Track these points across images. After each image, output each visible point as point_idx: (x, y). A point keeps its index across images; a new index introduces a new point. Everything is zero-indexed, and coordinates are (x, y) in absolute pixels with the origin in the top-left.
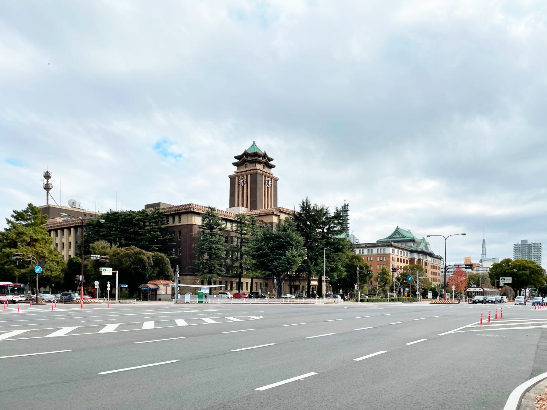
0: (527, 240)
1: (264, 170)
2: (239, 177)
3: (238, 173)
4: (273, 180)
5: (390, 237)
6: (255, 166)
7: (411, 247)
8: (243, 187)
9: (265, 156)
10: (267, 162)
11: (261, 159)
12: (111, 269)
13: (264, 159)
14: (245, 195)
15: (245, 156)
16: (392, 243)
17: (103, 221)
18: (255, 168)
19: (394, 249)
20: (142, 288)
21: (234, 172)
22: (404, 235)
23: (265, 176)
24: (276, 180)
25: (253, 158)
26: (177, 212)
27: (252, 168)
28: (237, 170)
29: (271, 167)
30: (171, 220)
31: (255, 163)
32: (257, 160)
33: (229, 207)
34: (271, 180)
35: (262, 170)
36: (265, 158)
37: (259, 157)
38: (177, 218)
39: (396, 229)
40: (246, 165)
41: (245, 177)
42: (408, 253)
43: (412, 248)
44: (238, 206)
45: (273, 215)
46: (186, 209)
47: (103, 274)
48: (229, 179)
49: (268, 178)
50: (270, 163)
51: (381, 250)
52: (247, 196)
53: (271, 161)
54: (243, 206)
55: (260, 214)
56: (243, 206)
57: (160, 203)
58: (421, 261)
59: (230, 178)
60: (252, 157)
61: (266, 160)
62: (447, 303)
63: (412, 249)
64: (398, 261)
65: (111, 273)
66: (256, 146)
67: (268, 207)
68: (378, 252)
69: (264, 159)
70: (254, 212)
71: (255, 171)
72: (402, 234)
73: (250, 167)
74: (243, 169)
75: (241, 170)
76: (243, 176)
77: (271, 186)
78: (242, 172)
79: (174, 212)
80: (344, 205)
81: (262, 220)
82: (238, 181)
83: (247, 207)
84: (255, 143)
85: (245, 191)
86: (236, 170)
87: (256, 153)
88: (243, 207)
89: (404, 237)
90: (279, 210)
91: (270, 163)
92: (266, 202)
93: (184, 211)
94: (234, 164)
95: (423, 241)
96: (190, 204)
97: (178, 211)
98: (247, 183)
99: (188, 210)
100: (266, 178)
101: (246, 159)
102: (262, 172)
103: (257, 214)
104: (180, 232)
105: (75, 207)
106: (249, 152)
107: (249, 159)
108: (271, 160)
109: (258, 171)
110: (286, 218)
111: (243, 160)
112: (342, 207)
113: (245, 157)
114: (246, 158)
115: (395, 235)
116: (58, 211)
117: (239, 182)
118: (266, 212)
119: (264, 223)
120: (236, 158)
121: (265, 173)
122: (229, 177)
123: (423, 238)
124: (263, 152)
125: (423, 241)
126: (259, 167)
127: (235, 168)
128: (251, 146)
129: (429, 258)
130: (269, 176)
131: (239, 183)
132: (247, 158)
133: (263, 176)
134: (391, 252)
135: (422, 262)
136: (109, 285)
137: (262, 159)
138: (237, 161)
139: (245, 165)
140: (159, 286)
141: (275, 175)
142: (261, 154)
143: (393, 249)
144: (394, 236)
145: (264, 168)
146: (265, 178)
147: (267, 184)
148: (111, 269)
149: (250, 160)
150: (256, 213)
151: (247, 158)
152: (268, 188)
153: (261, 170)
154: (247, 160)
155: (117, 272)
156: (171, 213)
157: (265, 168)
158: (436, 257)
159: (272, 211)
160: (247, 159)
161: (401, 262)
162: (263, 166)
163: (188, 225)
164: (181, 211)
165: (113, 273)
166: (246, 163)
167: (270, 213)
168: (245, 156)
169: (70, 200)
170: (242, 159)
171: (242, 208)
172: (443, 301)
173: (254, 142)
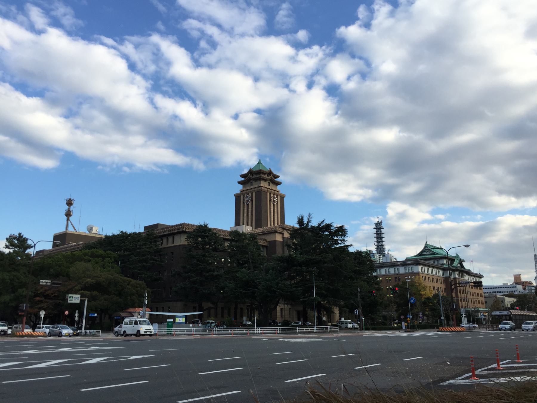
0: (144, 227)
3: (243, 191)
4: (279, 197)
5: (420, 254)
6: (260, 183)
7: (444, 264)
8: (248, 205)
9: (270, 173)
10: (273, 179)
11: (266, 176)
12: (79, 296)
13: (269, 176)
14: (250, 213)
16: (420, 260)
17: (58, 243)
21: (240, 190)
22: (434, 252)
23: (270, 194)
24: (282, 198)
26: (170, 232)
27: (256, 186)
28: (243, 188)
29: (278, 183)
30: (165, 241)
31: (260, 181)
32: (262, 177)
34: (277, 197)
35: (267, 187)
36: (270, 175)
37: (264, 174)
38: (170, 239)
39: (425, 245)
40: (251, 183)
41: (250, 195)
42: (441, 271)
43: (445, 266)
44: (243, 224)
45: (276, 233)
46: (179, 229)
47: (69, 302)
48: (235, 198)
49: (274, 195)
50: (277, 180)
51: (409, 269)
52: (252, 214)
54: (248, 225)
55: (263, 232)
57: (158, 224)
58: (457, 280)
60: (257, 175)
61: (272, 177)
62: (446, 330)
63: (445, 267)
64: (429, 281)
65: (78, 300)
66: (261, 164)
69: (269, 176)
70: (259, 230)
72: (433, 251)
73: (255, 185)
74: (248, 187)
75: (246, 189)
76: (248, 194)
77: (277, 204)
78: (247, 190)
80: (377, 222)
82: (244, 199)
83: (252, 226)
84: (261, 161)
85: (250, 209)
86: (242, 188)
87: (261, 170)
90: (282, 227)
91: (277, 180)
92: (272, 219)
93: (177, 231)
94: (240, 183)
95: (457, 257)
96: (183, 224)
98: (252, 201)
99: (180, 230)
100: (272, 195)
102: (267, 189)
103: (260, 233)
104: (172, 253)
105: (92, 232)
106: (254, 170)
107: (255, 176)
108: (277, 177)
109: (262, 188)
111: (248, 178)
112: (376, 225)
113: (250, 175)
114: (251, 176)
115: (424, 252)
116: (77, 237)
117: (244, 200)
118: (269, 230)
119: (267, 241)
120: (242, 176)
121: (270, 190)
123: (456, 254)
124: (269, 169)
125: (457, 257)
126: (263, 184)
127: (241, 187)
128: (257, 165)
130: (275, 193)
131: (244, 201)
132: (253, 176)
133: (268, 194)
134: (420, 271)
136: (77, 315)
137: (268, 176)
138: (243, 179)
139: (250, 182)
142: (267, 172)
143: (422, 267)
144: (424, 253)
145: (269, 185)
146: (270, 195)
147: (272, 201)
148: (79, 296)
149: (255, 178)
150: (259, 232)
151: (253, 176)
152: (274, 205)
153: (266, 188)
155: (87, 299)
156: (165, 233)
158: (475, 275)
159: (274, 229)
160: (252, 177)
161: (433, 281)
162: (269, 183)
163: (180, 245)
164: (173, 232)
165: (81, 300)
166: (252, 181)
167: (272, 231)
169: (88, 226)
172: (446, 328)
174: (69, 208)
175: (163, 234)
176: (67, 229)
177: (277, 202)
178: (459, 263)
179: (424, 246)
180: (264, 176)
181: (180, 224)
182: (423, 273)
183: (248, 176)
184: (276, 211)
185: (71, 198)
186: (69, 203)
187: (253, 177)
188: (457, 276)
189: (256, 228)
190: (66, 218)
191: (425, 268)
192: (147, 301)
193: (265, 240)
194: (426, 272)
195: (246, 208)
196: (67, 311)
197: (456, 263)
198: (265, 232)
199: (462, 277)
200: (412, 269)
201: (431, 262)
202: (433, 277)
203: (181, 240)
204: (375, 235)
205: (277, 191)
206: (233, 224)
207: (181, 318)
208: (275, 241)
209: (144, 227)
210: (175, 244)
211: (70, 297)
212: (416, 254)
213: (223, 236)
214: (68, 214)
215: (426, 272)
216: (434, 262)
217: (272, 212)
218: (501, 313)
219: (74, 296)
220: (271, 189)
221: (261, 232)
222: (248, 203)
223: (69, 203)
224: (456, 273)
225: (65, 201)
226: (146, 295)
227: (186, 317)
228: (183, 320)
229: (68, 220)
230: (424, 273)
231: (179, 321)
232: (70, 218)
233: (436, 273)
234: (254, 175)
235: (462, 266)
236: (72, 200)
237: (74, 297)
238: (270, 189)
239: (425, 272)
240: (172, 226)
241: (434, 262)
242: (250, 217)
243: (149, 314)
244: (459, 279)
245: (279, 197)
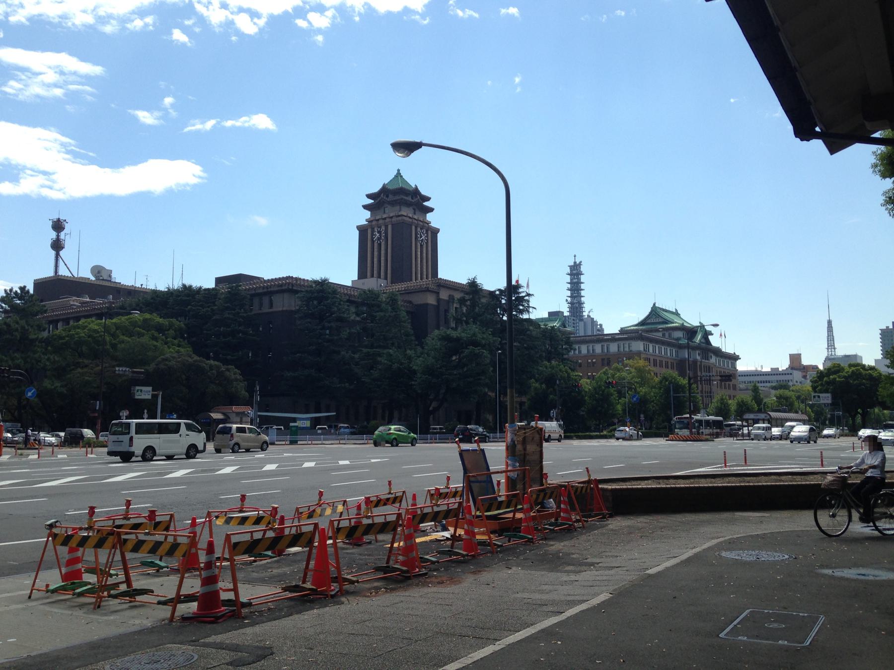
1: (416, 217)
4: (430, 233)
8: (380, 245)
9: (416, 192)
12: (150, 389)
15: (382, 194)
18: (400, 214)
19: (647, 344)
20: (201, 419)
23: (416, 228)
25: (397, 197)
26: (265, 290)
33: (357, 279)
41: (383, 228)
44: (372, 276)
47: (137, 397)
48: (358, 232)
50: (426, 204)
53: (427, 201)
55: (407, 290)
56: (379, 277)
58: (699, 364)
59: (358, 229)
60: (394, 196)
65: (149, 395)
66: (401, 176)
67: (427, 278)
68: (620, 350)
71: (400, 218)
72: (662, 318)
75: (378, 218)
76: (381, 228)
77: (427, 243)
79: (261, 291)
80: (573, 264)
81: (410, 300)
82: (372, 234)
83: (386, 278)
84: (401, 172)
85: (383, 252)
88: (379, 279)
89: (667, 323)
91: (426, 204)
92: (419, 269)
94: (366, 207)
97: (268, 288)
99: (284, 288)
100: (419, 229)
101: (385, 200)
102: (411, 220)
103: (401, 291)
106: (390, 187)
107: (391, 198)
108: (428, 199)
110: (450, 295)
113: (384, 196)
120: (369, 196)
121: (416, 222)
122: (359, 228)
124: (414, 186)
126: (406, 212)
127: (367, 214)
128: (394, 178)
130: (423, 226)
133: (413, 227)
135: (700, 366)
137: (412, 198)
138: (371, 201)
140: (229, 415)
141: (433, 224)
142: (409, 191)
143: (645, 343)
144: (649, 321)
145: (415, 214)
151: (387, 196)
152: (421, 245)
153: (410, 218)
154: (387, 200)
155: (161, 393)
157: (416, 212)
161: (661, 366)
162: (414, 209)
164: (272, 289)
165: (153, 396)
168: (382, 194)
170: (379, 199)
171: (377, 280)
173: (399, 170)
174: (58, 236)
175: (254, 292)
176: (56, 272)
177: (427, 240)
179: (649, 310)
180: (406, 198)
181: (283, 277)
182: (646, 353)
183: (380, 198)
184: (425, 255)
185: (61, 218)
186: (58, 226)
188: (698, 358)
190: (53, 253)
192: (259, 396)
194: (651, 350)
196: (128, 413)
197: (699, 338)
198: (410, 290)
199: (705, 359)
200: (629, 347)
202: (661, 359)
204: (569, 286)
205: (426, 223)
207: (305, 422)
208: (427, 304)
209: (216, 278)
211: (138, 391)
212: (636, 322)
214: (57, 246)
215: (651, 350)
217: (419, 256)
218: (756, 416)
219: (144, 388)
220: (417, 220)
221: (403, 291)
222: (380, 241)
223: (58, 226)
224: (697, 352)
225: (51, 223)
226: (256, 389)
227: (311, 418)
228: (307, 424)
229: (57, 256)
230: (649, 353)
231: (302, 426)
232: (62, 253)
233: (666, 353)
234: (390, 196)
235: (708, 342)
236: (62, 221)
237: (143, 390)
238: (415, 219)
239: (650, 351)
242: (383, 264)
244: (701, 362)
245: (430, 233)
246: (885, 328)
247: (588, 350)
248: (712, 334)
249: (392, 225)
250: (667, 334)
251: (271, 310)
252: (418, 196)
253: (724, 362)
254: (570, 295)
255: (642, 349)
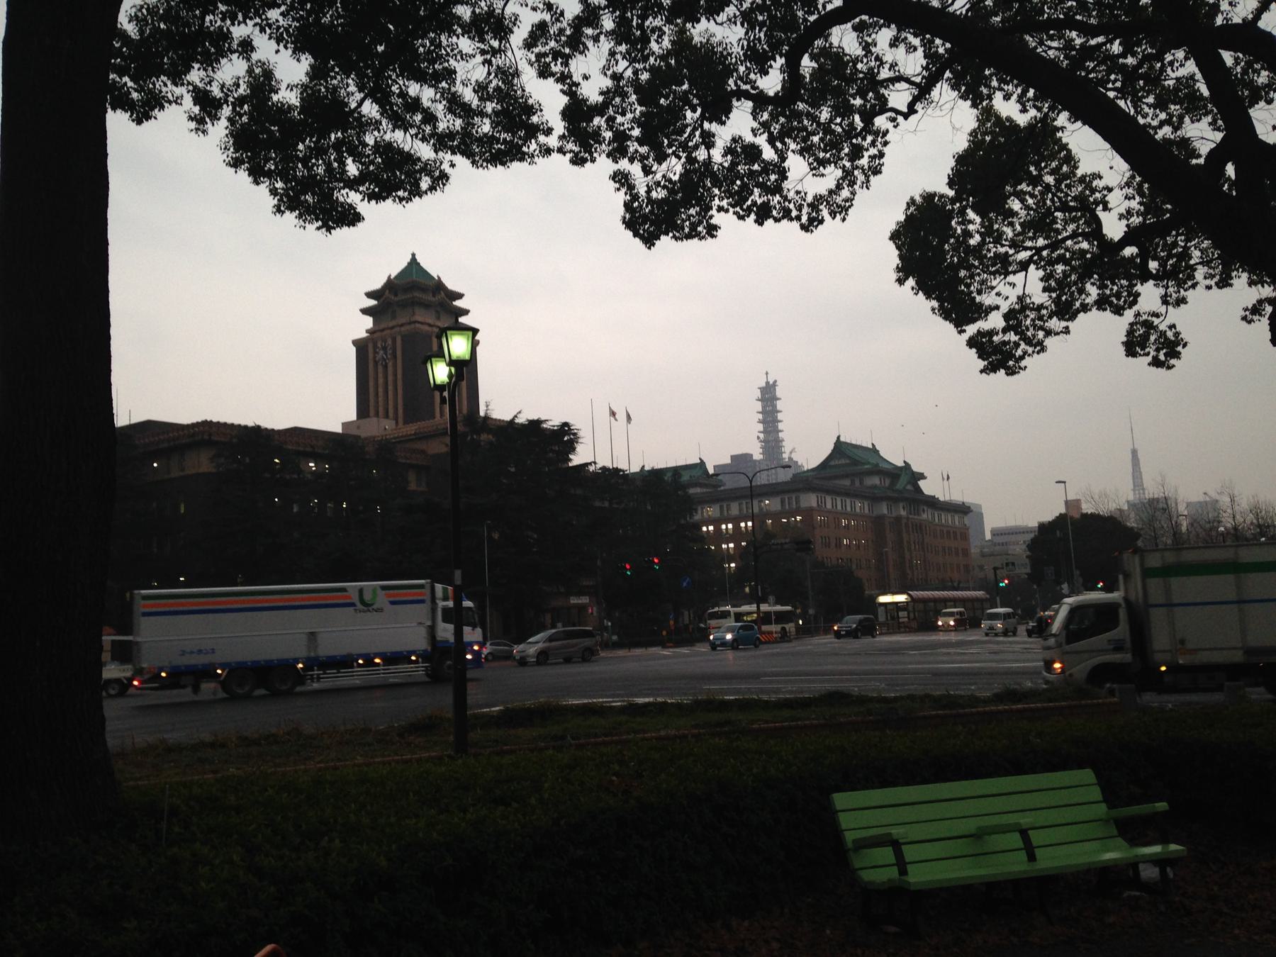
2: (375, 346)
8: (386, 367)
9: (439, 286)
15: (387, 291)
25: (409, 296)
26: (172, 444)
41: (390, 342)
48: (354, 349)
50: (458, 303)
58: (904, 521)
70: (411, 429)
71: (413, 326)
75: (383, 326)
79: (166, 445)
82: (375, 353)
84: (416, 257)
85: (390, 378)
89: (856, 465)
91: (458, 303)
94: (365, 311)
98: (395, 357)
103: (411, 435)
107: (401, 297)
108: (460, 296)
109: (417, 325)
120: (370, 295)
122: (355, 343)
127: (368, 322)
129: (926, 515)
135: (907, 525)
137: (434, 296)
138: (372, 302)
144: (832, 463)
151: (396, 295)
153: (430, 325)
162: (437, 312)
173: (413, 255)
178: (909, 483)
179: (832, 447)
187: (396, 299)
188: (903, 513)
189: (405, 423)
191: (827, 497)
193: (423, 452)
194: (829, 506)
195: (380, 375)
197: (902, 483)
201: (847, 482)
203: (202, 463)
204: (760, 416)
206: (352, 415)
210: (188, 472)
213: (312, 447)
215: (829, 506)
216: (853, 482)
224: (901, 505)
235: (919, 490)
240: (188, 426)
241: (853, 482)
243: (113, 641)
246: (729, 461)
247: (740, 510)
248: (925, 478)
249: (402, 337)
250: (857, 483)
251: (182, 474)
252: (442, 292)
253: (940, 516)
254: (762, 429)
255: (814, 504)
